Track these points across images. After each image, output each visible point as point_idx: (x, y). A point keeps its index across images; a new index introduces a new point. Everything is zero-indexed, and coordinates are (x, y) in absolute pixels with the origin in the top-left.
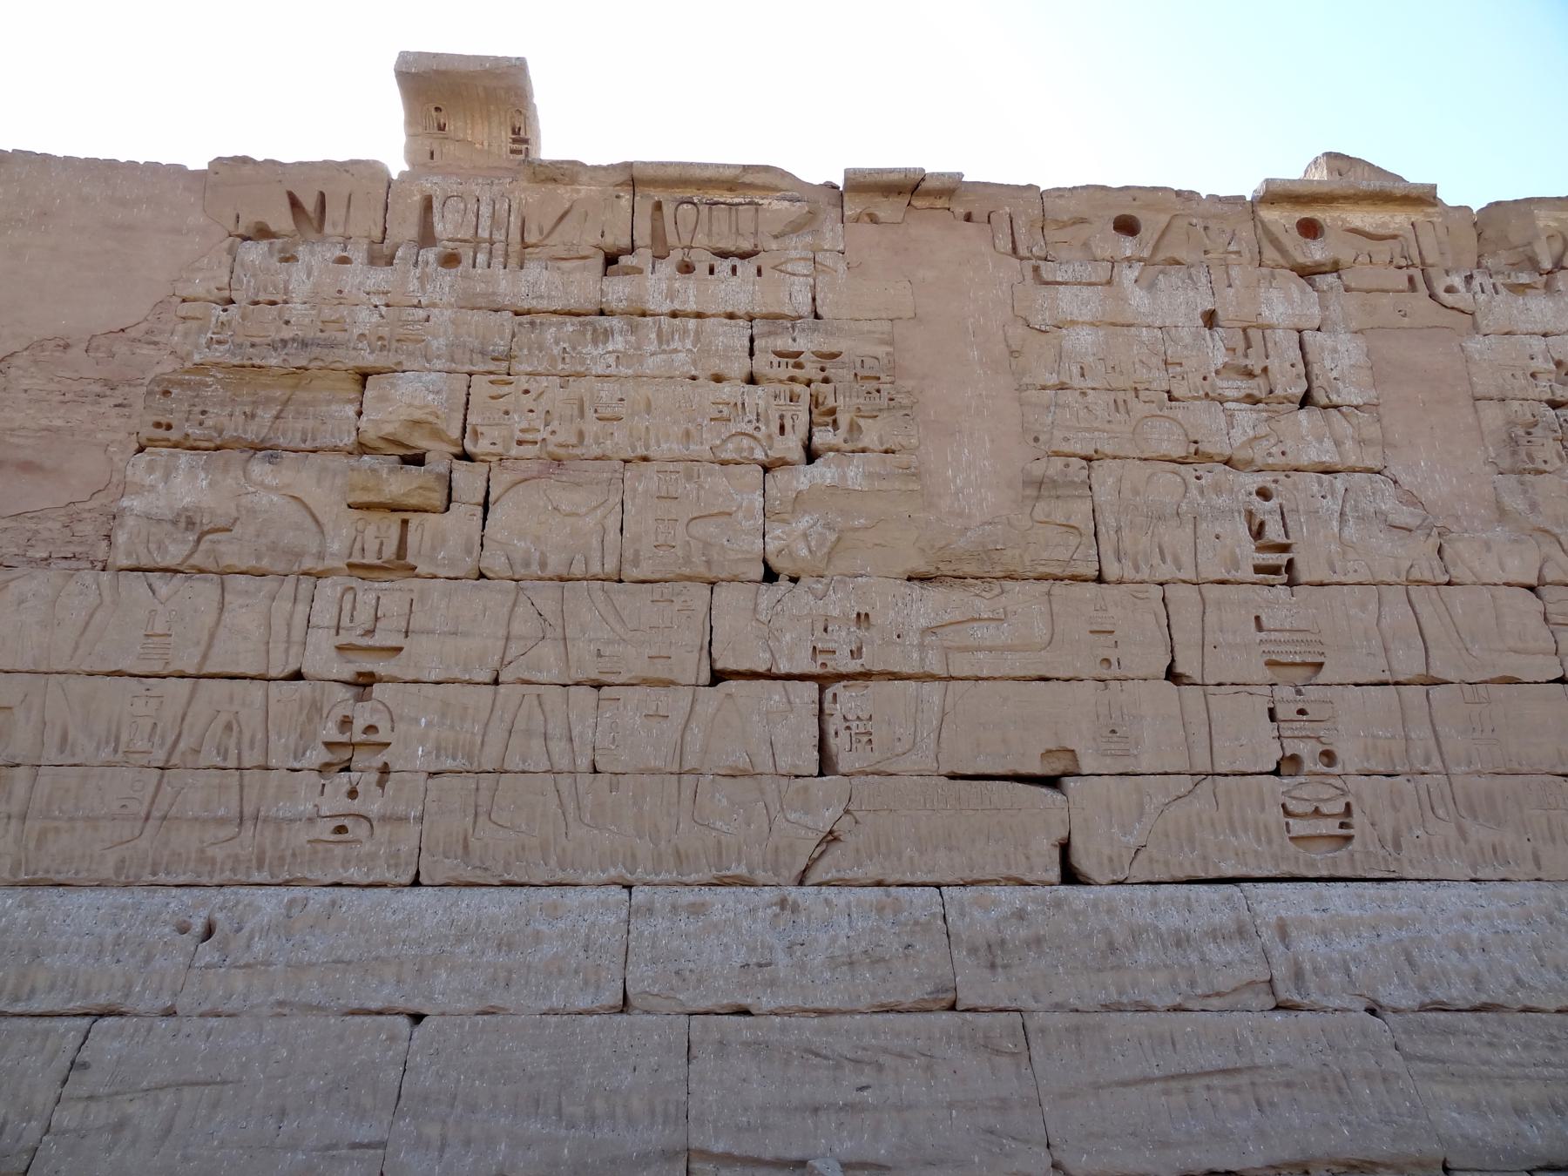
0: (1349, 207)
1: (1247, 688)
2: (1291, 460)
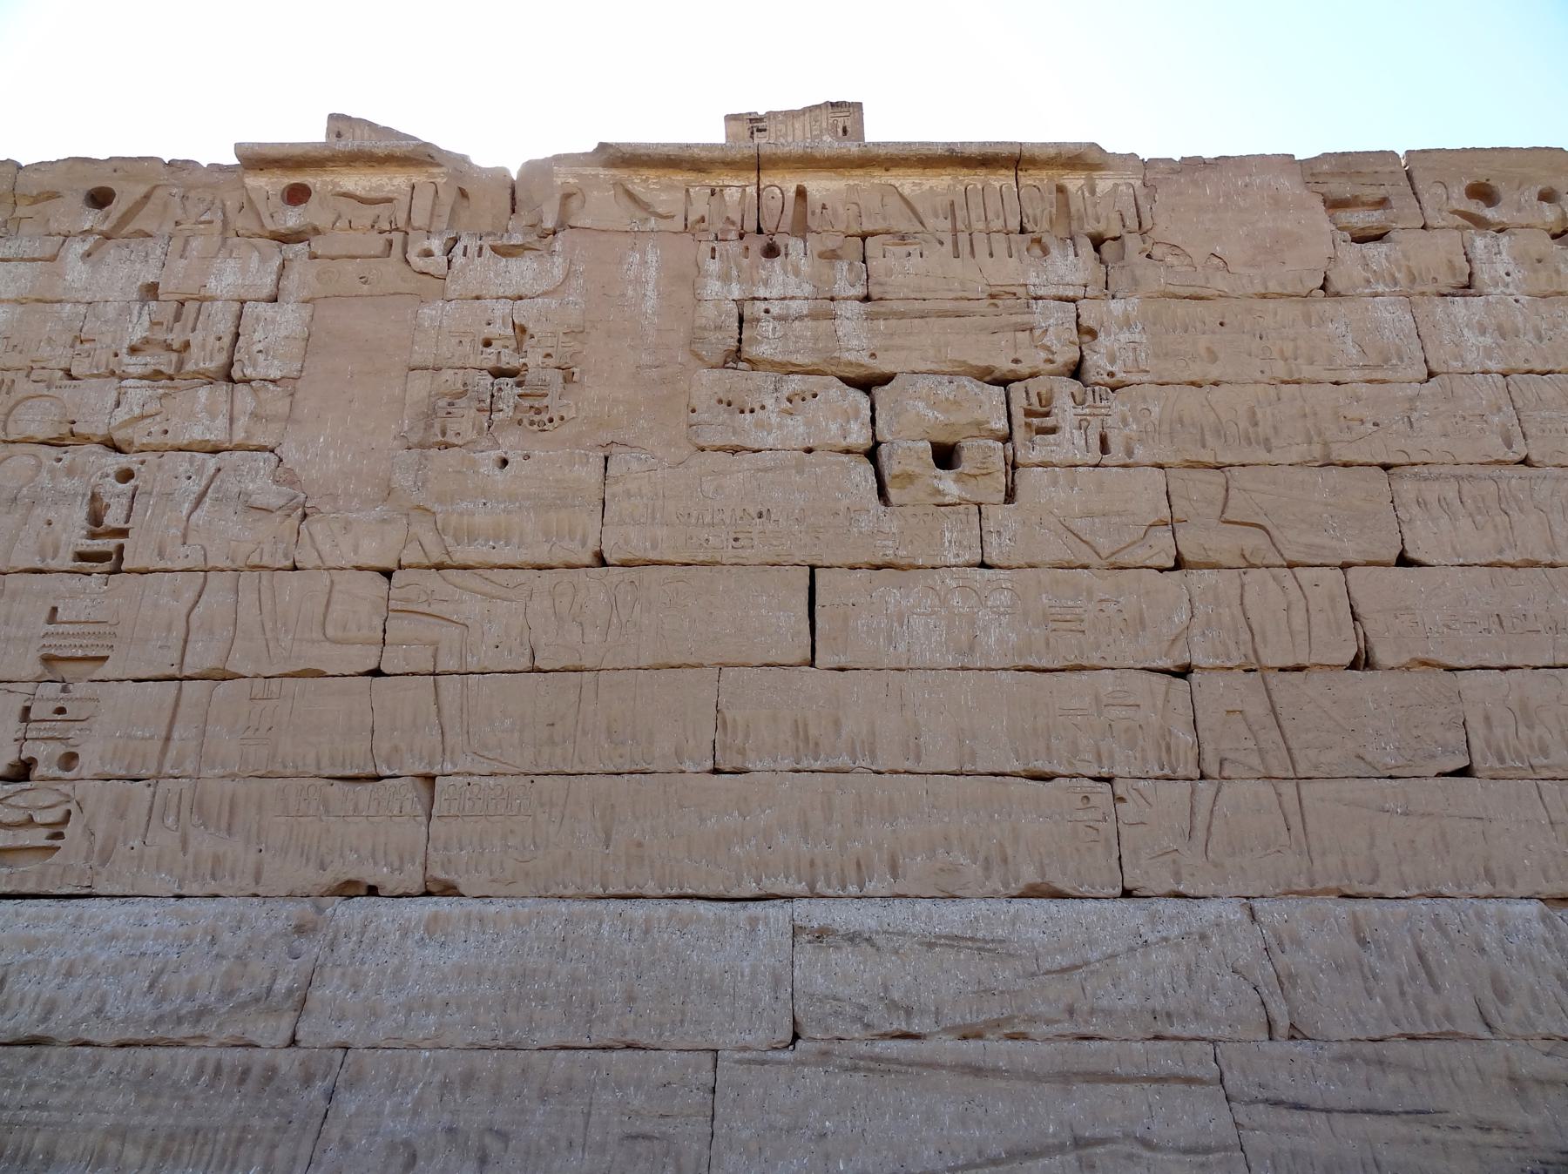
0: (345, 170)
1: (8, 686)
2: (169, 440)
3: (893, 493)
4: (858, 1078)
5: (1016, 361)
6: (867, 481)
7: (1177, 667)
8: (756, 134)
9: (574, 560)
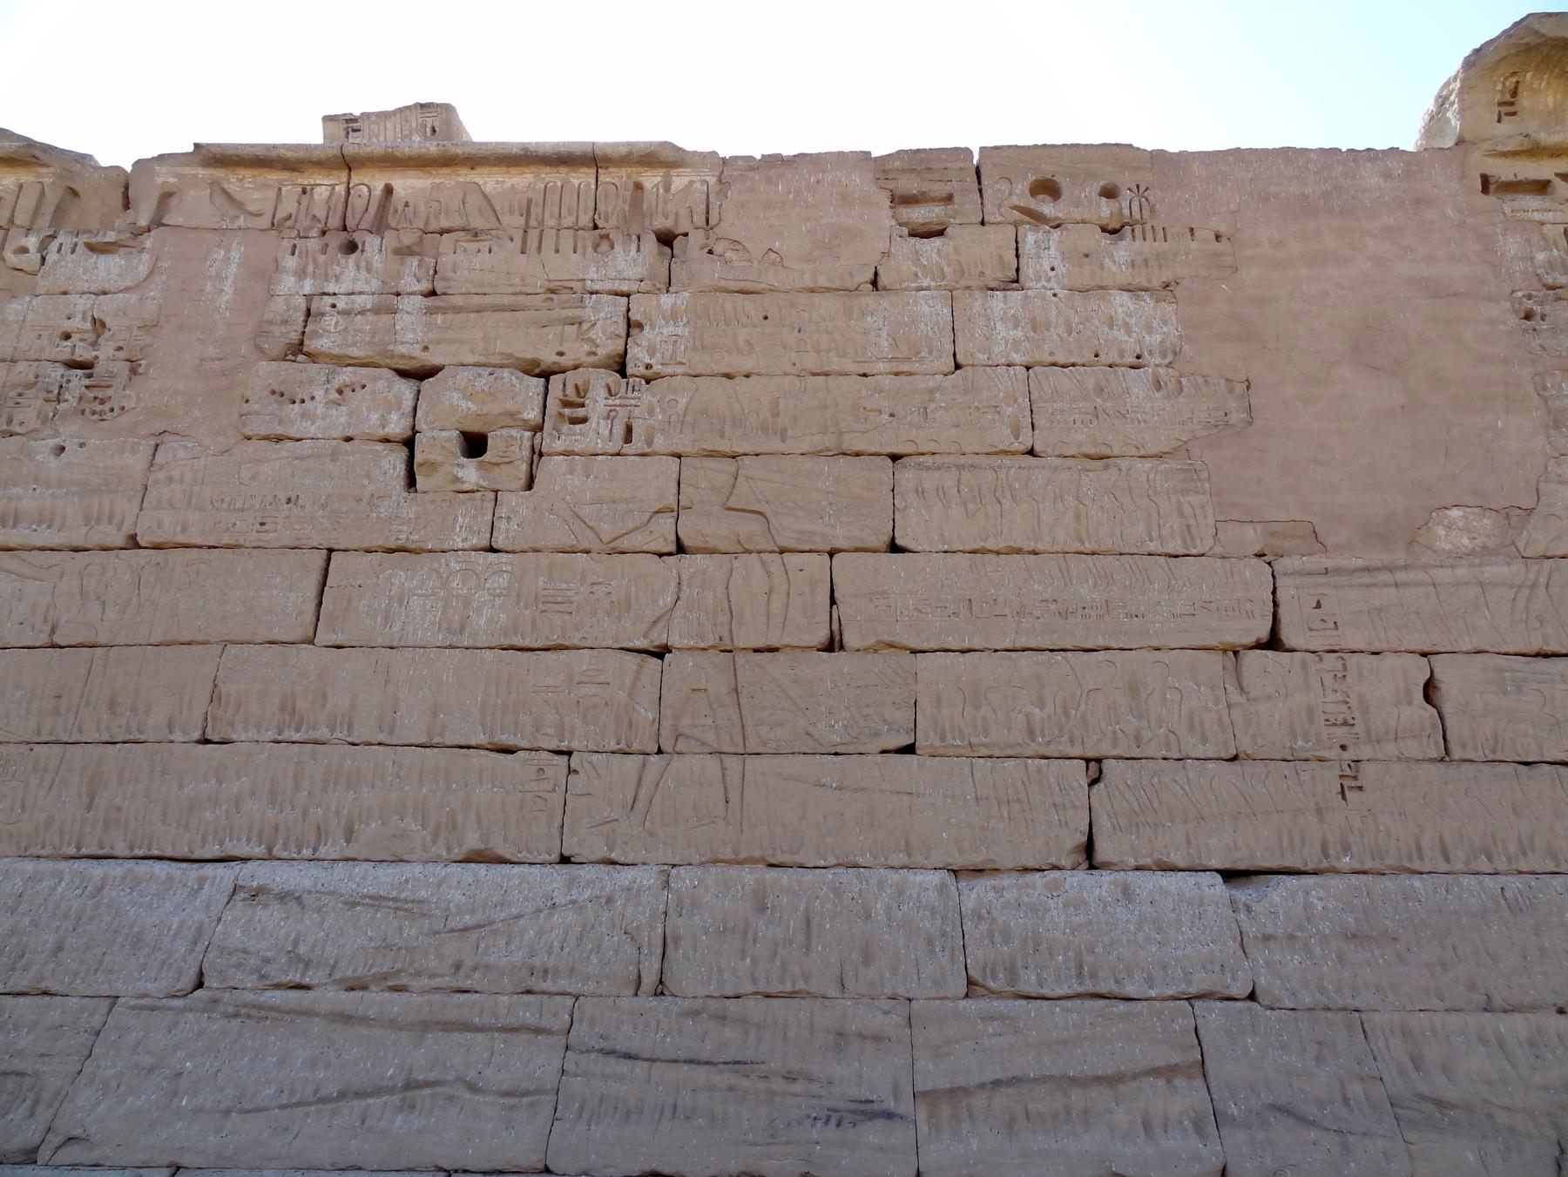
3: (420, 480)
4: (236, 1022)
5: (561, 354)
6: (394, 469)
7: (657, 647)
8: (351, 134)
9: (108, 542)
